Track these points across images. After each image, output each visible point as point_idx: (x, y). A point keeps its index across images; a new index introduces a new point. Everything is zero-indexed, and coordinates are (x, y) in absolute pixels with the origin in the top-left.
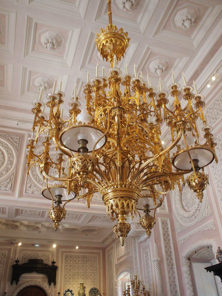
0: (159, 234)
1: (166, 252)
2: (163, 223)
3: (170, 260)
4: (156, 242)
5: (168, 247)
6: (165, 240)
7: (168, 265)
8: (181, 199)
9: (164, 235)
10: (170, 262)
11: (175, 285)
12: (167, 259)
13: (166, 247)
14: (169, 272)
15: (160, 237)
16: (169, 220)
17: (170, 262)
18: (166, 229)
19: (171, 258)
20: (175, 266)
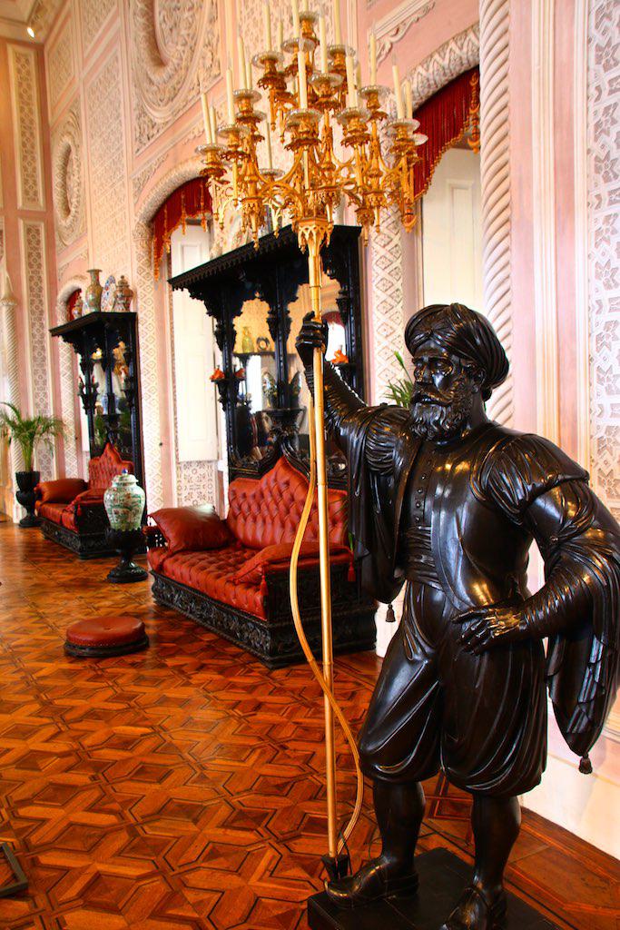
0: (18, 254)
1: (31, 289)
2: (28, 231)
3: (37, 303)
4: (9, 269)
5: (36, 279)
6: (30, 265)
7: (32, 312)
8: (65, 183)
9: (29, 255)
10: (37, 308)
11: (43, 349)
12: (32, 302)
13: (30, 279)
14: (33, 325)
15: (19, 259)
16: (43, 225)
17: (37, 308)
18: (34, 244)
19: (41, 301)
20: (46, 315)
